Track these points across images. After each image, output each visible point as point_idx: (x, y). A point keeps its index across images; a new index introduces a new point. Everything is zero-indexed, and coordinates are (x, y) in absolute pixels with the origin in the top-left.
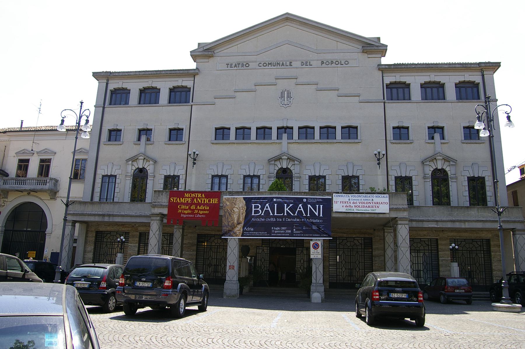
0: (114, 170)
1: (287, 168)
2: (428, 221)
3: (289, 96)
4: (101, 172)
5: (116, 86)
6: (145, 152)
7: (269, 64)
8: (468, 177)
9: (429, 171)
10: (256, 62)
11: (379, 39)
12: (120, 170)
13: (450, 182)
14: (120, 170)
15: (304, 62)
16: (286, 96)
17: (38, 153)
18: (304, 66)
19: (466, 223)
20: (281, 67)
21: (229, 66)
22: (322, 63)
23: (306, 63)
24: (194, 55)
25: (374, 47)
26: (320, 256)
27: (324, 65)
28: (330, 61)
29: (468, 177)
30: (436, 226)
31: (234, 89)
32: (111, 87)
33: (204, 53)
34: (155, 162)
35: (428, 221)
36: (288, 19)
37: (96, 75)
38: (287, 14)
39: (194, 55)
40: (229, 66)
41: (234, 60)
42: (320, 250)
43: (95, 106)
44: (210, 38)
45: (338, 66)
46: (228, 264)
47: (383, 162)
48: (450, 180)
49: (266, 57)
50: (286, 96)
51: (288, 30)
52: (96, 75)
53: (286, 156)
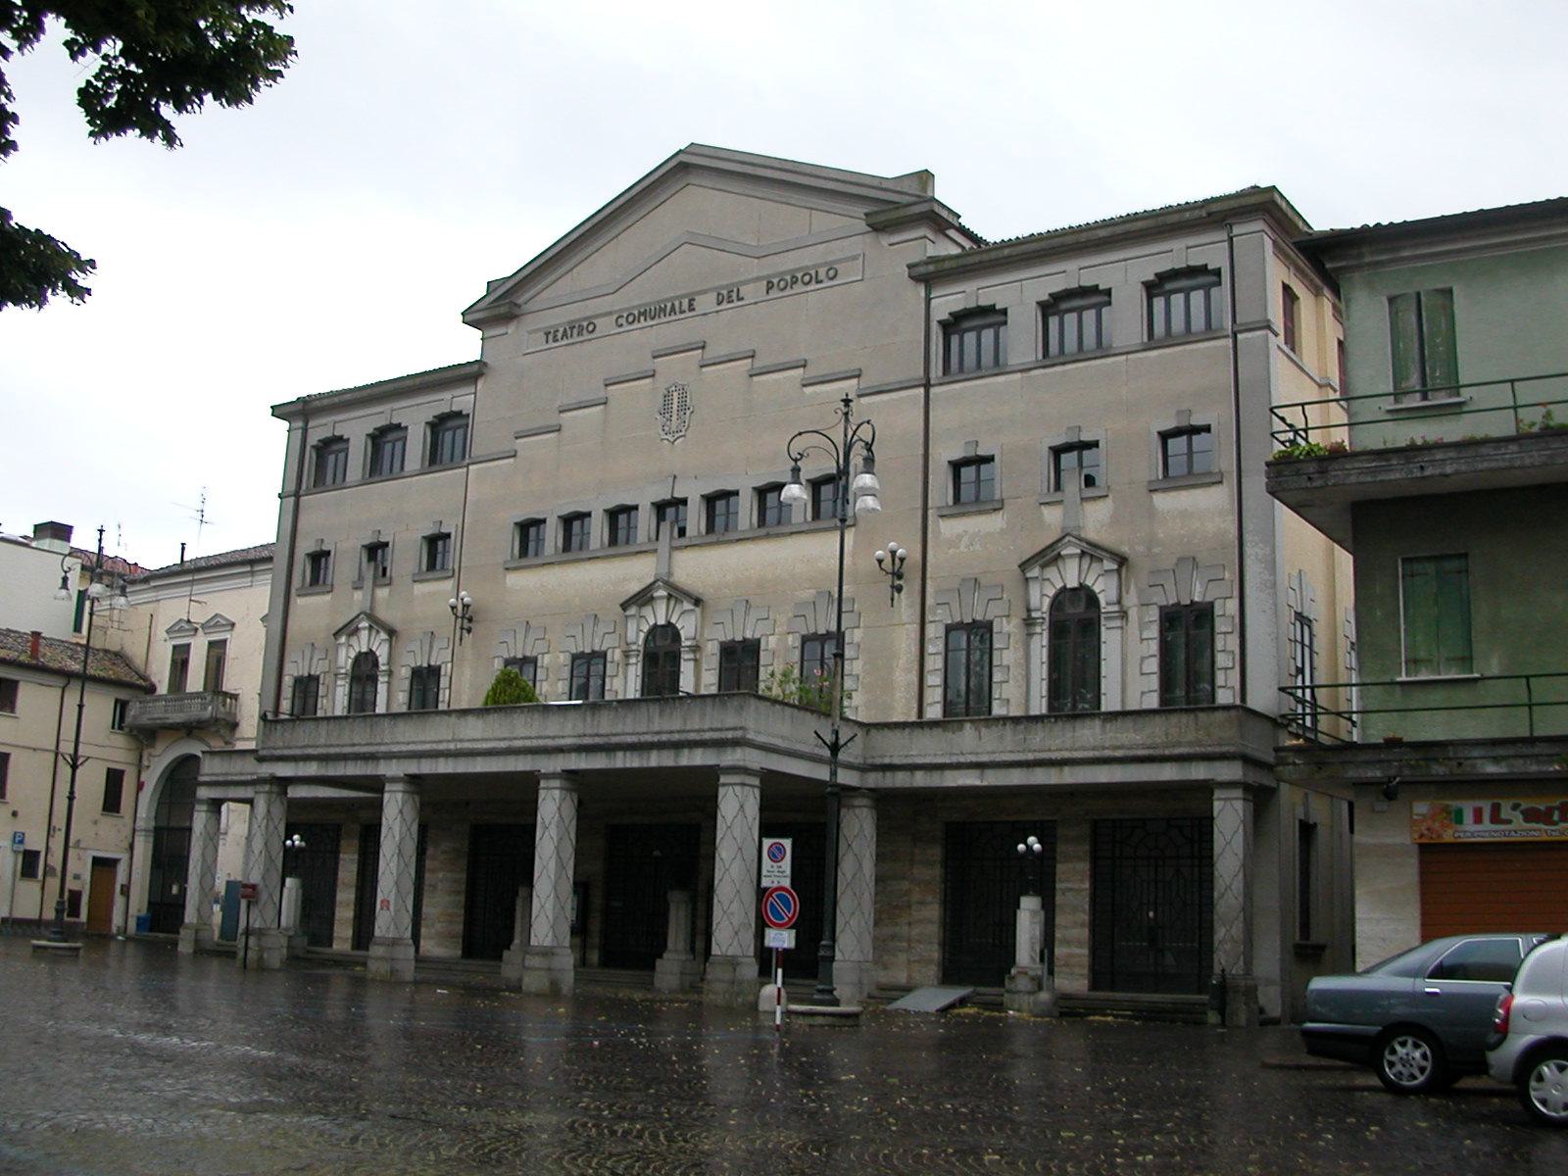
0: (434, 654)
1: (1082, 587)
2: (958, 766)
3: (683, 407)
4: (292, 671)
5: (326, 433)
6: (372, 608)
7: (640, 314)
8: (1161, 608)
9: (1041, 598)
10: (610, 313)
11: (925, 177)
12: (327, 661)
13: (1103, 629)
14: (327, 661)
15: (725, 292)
16: (675, 407)
17: (203, 626)
18: (725, 306)
19: (1066, 769)
20: (668, 318)
21: (551, 337)
22: (770, 286)
23: (729, 295)
24: (475, 317)
25: (905, 208)
26: (787, 883)
27: (774, 293)
28: (788, 278)
29: (1161, 608)
30: (978, 783)
31: (559, 403)
32: (314, 438)
33: (498, 308)
34: (392, 633)
35: (958, 766)
36: (688, 168)
37: (278, 411)
38: (693, 149)
39: (475, 317)
40: (551, 337)
41: (559, 318)
42: (786, 864)
43: (280, 496)
44: (507, 266)
45: (809, 288)
46: (380, 897)
47: (911, 586)
48: (1103, 622)
49: (635, 296)
50: (675, 407)
51: (697, 201)
52: (278, 411)
53: (1075, 545)
